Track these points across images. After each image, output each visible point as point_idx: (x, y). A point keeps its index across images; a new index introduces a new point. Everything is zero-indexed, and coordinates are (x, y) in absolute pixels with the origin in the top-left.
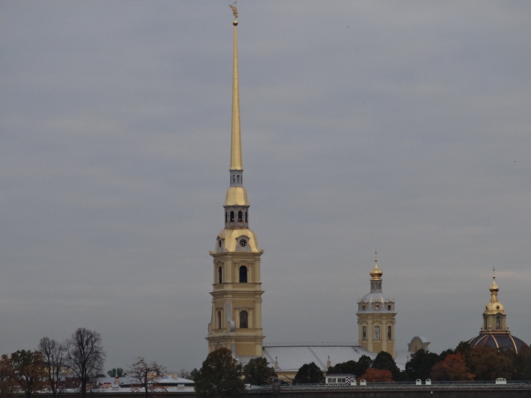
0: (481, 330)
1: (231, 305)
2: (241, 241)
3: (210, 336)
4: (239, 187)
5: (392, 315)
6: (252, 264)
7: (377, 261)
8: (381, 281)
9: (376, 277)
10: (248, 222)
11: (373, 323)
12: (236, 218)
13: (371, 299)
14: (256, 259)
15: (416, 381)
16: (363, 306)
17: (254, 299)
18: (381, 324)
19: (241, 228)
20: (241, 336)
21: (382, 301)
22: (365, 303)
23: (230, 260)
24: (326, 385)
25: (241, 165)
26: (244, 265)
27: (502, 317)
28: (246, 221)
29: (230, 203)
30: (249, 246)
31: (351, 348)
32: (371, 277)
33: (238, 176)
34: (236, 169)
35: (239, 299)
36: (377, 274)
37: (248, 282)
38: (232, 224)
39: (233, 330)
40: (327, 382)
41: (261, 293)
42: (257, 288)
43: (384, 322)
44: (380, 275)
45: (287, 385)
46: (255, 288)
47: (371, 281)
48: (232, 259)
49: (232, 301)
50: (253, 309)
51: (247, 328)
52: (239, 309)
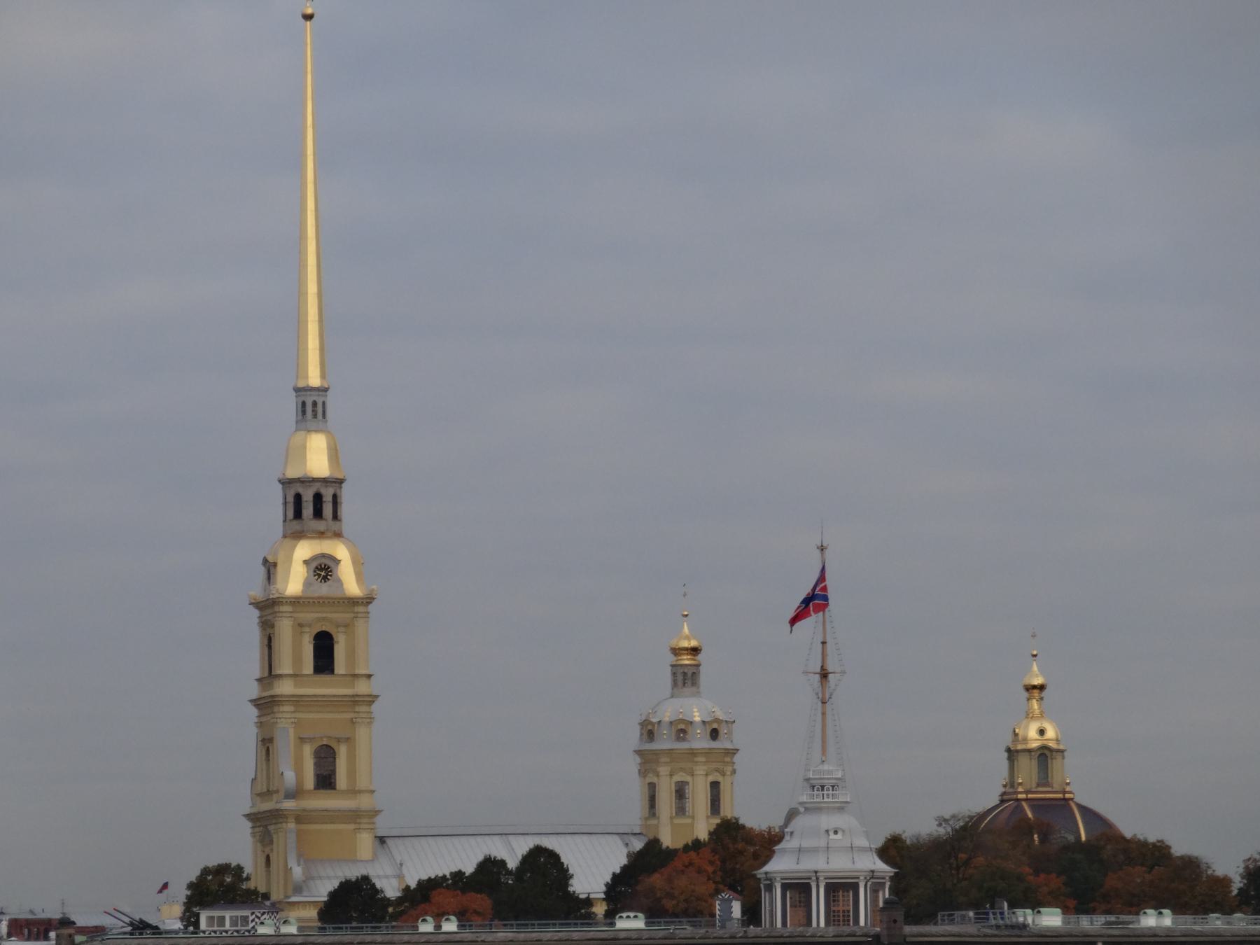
0: (1004, 790)
1: (291, 731)
2: (317, 568)
3: (254, 810)
4: (317, 431)
6: (346, 626)
7: (687, 615)
8: (698, 666)
9: (685, 657)
10: (340, 520)
11: (671, 775)
12: (308, 510)
13: (668, 712)
14: (357, 613)
15: (418, 922)
16: (649, 731)
18: (693, 775)
19: (321, 535)
21: (695, 716)
24: (202, 935)
25: (323, 376)
27: (1052, 755)
28: (336, 517)
29: (292, 473)
30: (339, 581)
31: (616, 838)
32: (671, 659)
33: (315, 404)
34: (308, 386)
35: (311, 716)
36: (686, 649)
37: (336, 672)
38: (296, 525)
39: (291, 795)
40: (203, 925)
41: (371, 699)
42: (362, 688)
43: (700, 770)
44: (695, 651)
45: (154, 934)
46: (354, 688)
47: (672, 666)
48: (292, 615)
49: (293, 720)
51: (334, 788)
52: (311, 740)
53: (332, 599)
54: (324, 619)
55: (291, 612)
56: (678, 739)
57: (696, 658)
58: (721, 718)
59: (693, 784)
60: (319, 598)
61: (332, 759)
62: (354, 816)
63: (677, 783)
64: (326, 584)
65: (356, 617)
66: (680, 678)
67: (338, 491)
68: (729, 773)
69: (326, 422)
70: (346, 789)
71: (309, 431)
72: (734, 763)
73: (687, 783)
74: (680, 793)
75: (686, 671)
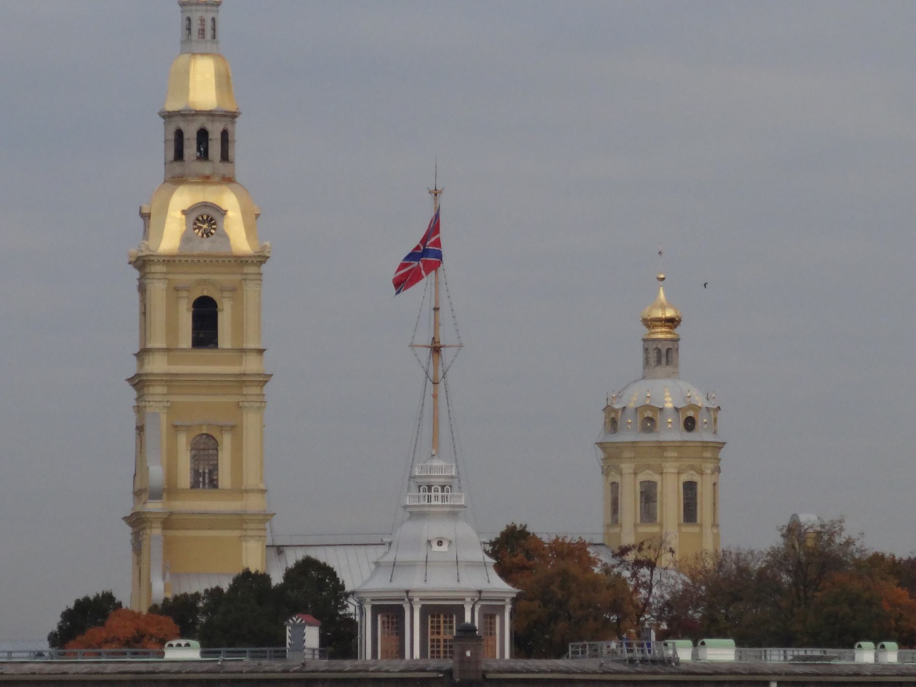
1: (164, 418)
2: (198, 219)
4: (203, 54)
5: (703, 447)
6: (234, 290)
7: (663, 279)
8: (676, 340)
9: (659, 330)
12: (191, 149)
13: (634, 398)
14: (246, 274)
17: (237, 398)
19: (206, 180)
21: (666, 402)
22: (616, 411)
23: (160, 279)
26: (205, 293)
29: (173, 106)
30: (225, 237)
32: (644, 331)
37: (220, 346)
38: (177, 168)
41: (263, 380)
42: (251, 365)
43: (670, 468)
44: (672, 322)
47: (645, 340)
49: (165, 404)
50: (235, 429)
52: (188, 428)
55: (164, 273)
58: (700, 405)
59: (662, 484)
61: (215, 451)
62: (239, 520)
66: (653, 356)
67: (229, 128)
68: (709, 471)
69: (217, 43)
71: (194, 54)
72: (719, 460)
74: (648, 495)
75: (659, 346)
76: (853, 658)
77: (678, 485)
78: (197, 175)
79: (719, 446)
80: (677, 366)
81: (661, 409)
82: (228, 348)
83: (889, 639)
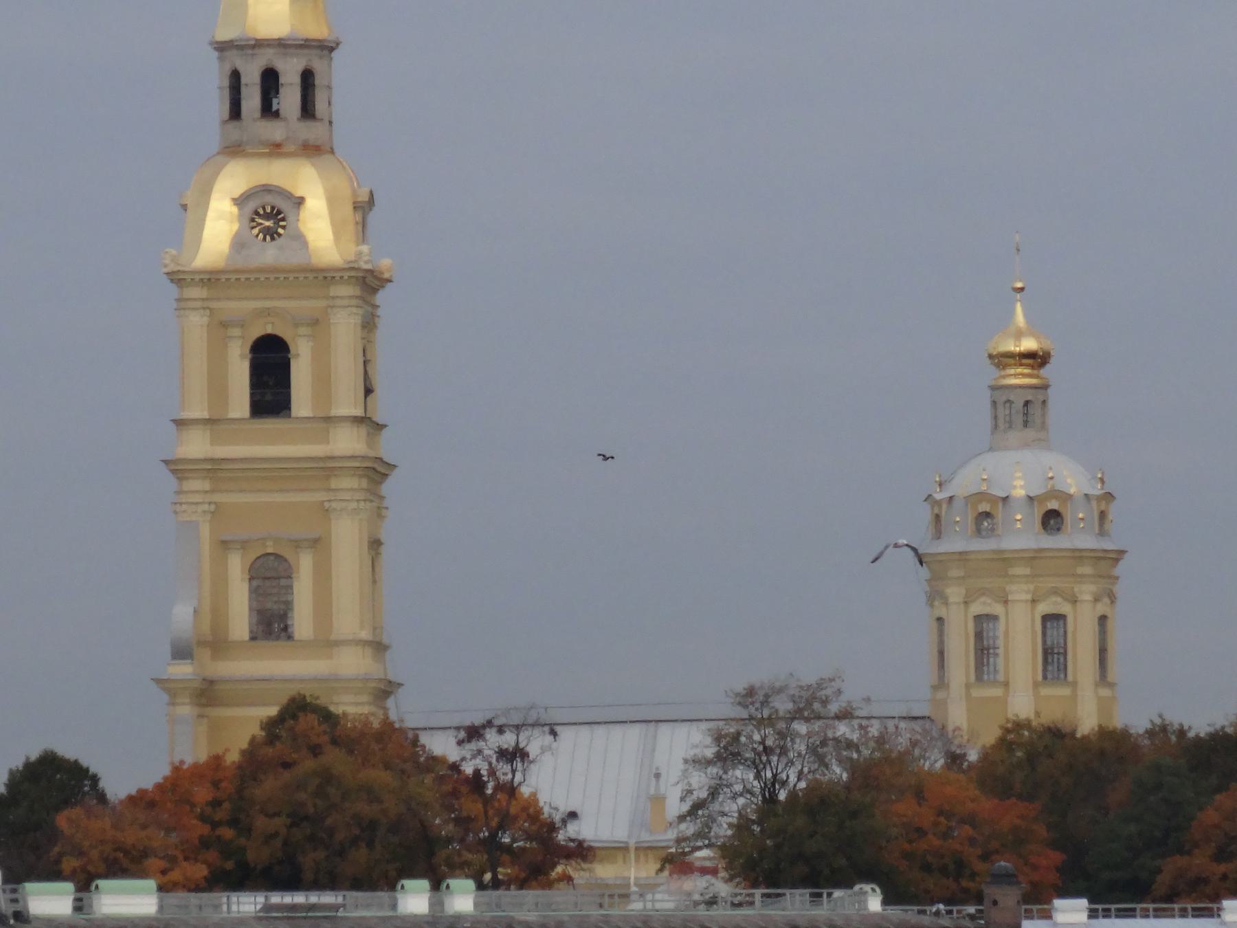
1: (205, 530)
5: (1074, 558)
6: (315, 323)
13: (965, 482)
14: (333, 298)
18: (1006, 602)
19: (276, 150)
20: (247, 681)
21: (1015, 487)
22: (938, 503)
29: (225, 34)
30: (301, 239)
32: (991, 374)
38: (234, 131)
43: (1020, 593)
46: (328, 443)
47: (993, 388)
48: (206, 304)
49: (206, 507)
50: (319, 544)
52: (244, 545)
53: (290, 271)
54: (268, 312)
55: (203, 300)
56: (978, 531)
57: (1044, 372)
58: (1072, 491)
60: (260, 270)
63: (978, 618)
64: (274, 243)
65: (332, 307)
67: (318, 66)
68: (1088, 597)
70: (312, 637)
73: (993, 618)
75: (1012, 398)
76: (394, 906)
77: (1033, 620)
78: (264, 143)
79: (1118, 556)
80: (1043, 426)
81: (1005, 499)
82: (306, 415)
83: (497, 869)
